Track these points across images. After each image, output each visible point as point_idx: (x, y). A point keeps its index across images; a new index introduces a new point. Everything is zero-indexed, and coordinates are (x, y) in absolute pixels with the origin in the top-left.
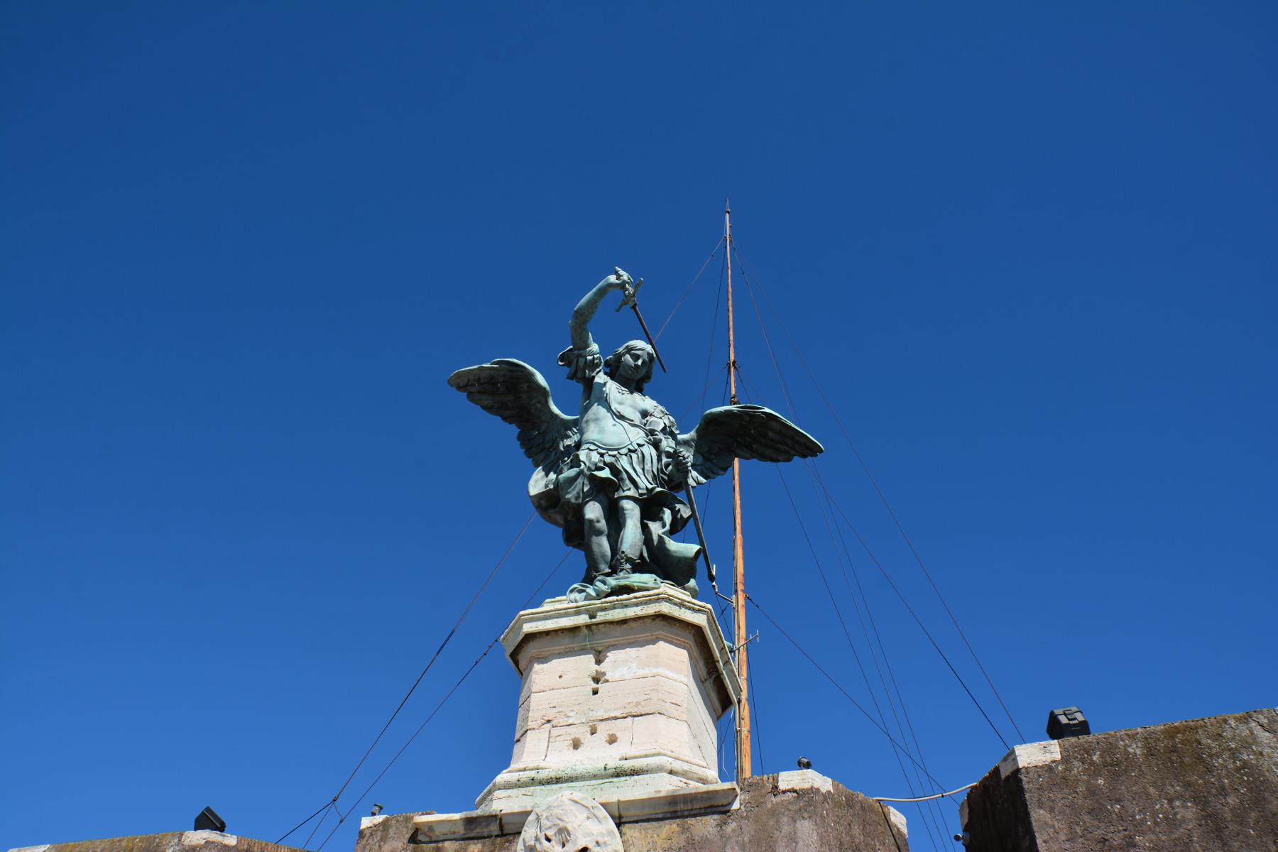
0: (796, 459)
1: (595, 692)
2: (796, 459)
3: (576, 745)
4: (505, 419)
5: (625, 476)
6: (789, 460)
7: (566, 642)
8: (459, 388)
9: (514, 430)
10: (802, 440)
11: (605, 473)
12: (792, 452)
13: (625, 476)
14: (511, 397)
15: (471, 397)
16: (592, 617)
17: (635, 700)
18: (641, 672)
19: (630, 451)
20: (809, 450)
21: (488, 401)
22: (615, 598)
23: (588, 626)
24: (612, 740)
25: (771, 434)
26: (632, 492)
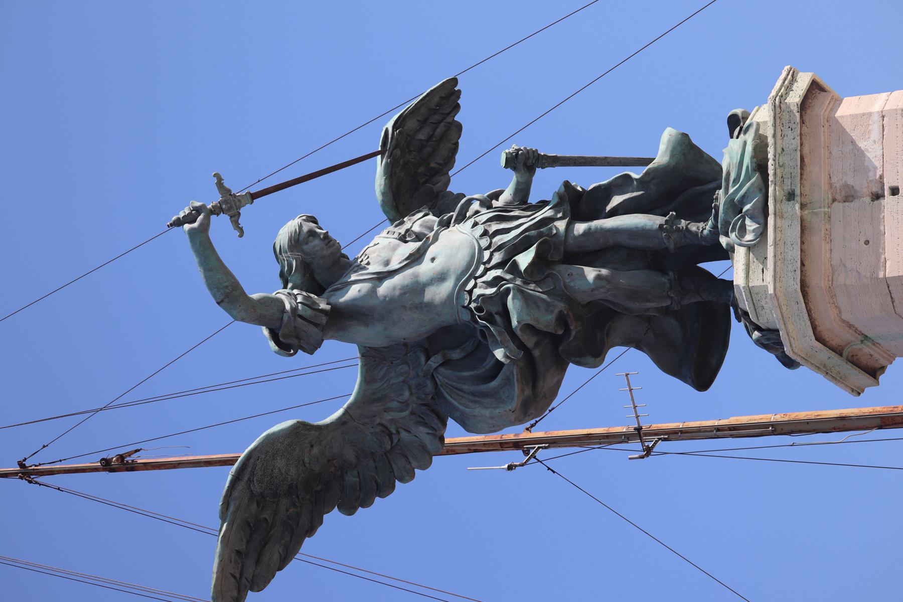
0: (458, 118)
1: (895, 191)
2: (458, 118)
4: (310, 531)
5: (533, 233)
6: (459, 127)
7: (816, 239)
9: (333, 518)
10: (436, 99)
11: (524, 260)
12: (449, 119)
13: (533, 233)
16: (791, 196)
19: (485, 233)
20: (446, 98)
21: (274, 552)
25: (421, 136)
26: (561, 225)
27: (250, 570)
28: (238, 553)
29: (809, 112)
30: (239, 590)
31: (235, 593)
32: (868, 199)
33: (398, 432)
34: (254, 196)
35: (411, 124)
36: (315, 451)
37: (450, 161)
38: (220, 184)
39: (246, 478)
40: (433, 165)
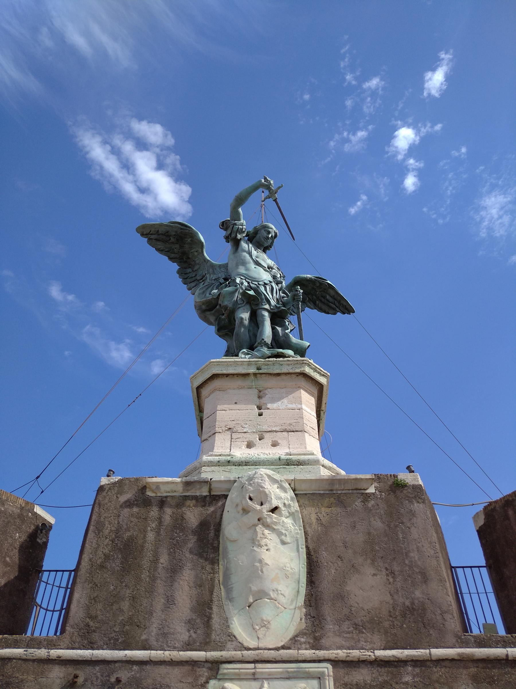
3: (250, 445)
4: (171, 259)
8: (142, 235)
9: (175, 267)
12: (337, 309)
14: (177, 246)
15: (150, 242)
17: (288, 422)
18: (290, 406)
22: (275, 359)
23: (255, 374)
24: (275, 444)
27: (153, 237)
28: (158, 231)
29: (303, 379)
30: (146, 234)
31: (145, 233)
32: (258, 404)
33: (203, 281)
34: (275, 200)
35: (332, 292)
36: (196, 254)
37: (321, 310)
38: (279, 188)
39: (182, 227)
40: (317, 302)
